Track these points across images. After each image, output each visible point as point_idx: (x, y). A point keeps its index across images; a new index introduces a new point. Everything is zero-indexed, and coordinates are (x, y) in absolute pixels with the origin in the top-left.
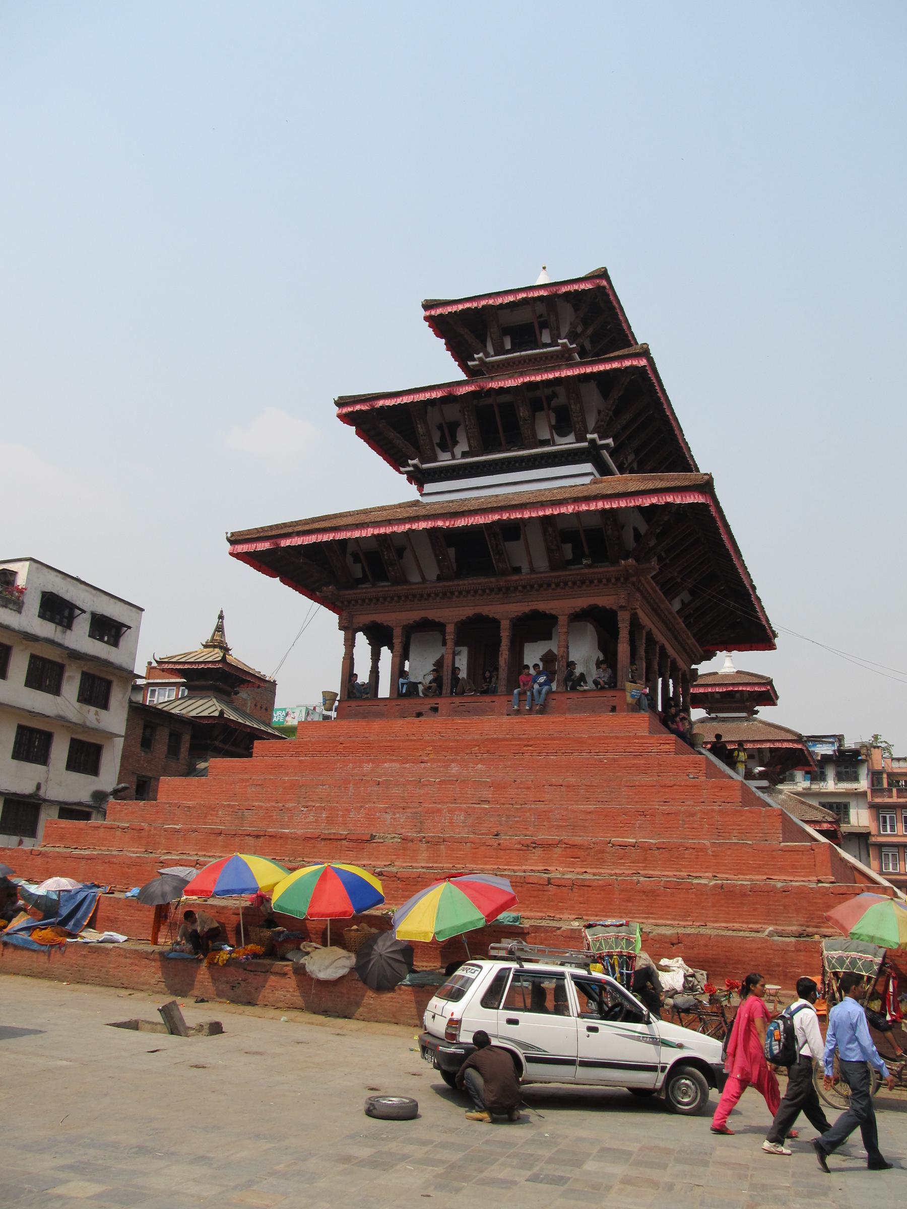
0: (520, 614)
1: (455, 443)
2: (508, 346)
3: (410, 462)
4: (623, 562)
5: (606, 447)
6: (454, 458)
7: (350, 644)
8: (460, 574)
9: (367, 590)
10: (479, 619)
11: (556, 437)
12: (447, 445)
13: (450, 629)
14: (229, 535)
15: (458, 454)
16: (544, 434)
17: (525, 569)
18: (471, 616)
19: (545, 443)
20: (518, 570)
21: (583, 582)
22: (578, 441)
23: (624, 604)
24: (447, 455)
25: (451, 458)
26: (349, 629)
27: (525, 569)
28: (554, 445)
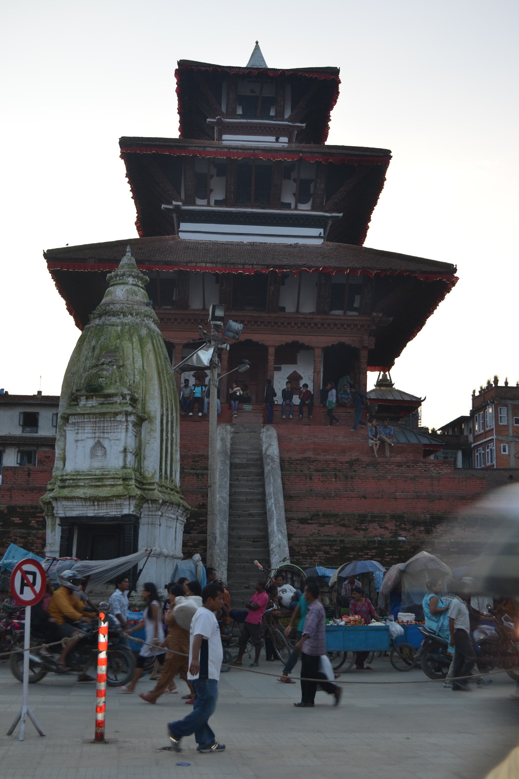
0: (284, 344)
2: (240, 111)
3: (174, 203)
4: (375, 314)
6: (209, 205)
10: (249, 342)
12: (205, 194)
14: (45, 252)
15: (212, 203)
16: (288, 198)
18: (243, 340)
19: (288, 206)
20: (283, 309)
22: (313, 209)
23: (367, 345)
24: (204, 202)
25: (206, 204)
28: (296, 209)
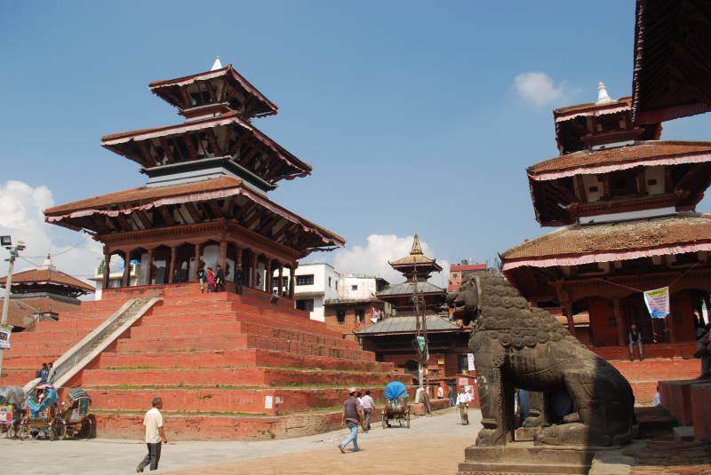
1: (162, 158)
2: (194, 103)
5: (229, 158)
6: (162, 164)
8: (153, 226)
9: (114, 235)
11: (208, 154)
12: (160, 158)
13: (150, 252)
17: (182, 222)
20: (178, 223)
21: (205, 229)
22: (216, 156)
24: (159, 164)
26: (108, 254)
27: (182, 222)
28: (207, 157)
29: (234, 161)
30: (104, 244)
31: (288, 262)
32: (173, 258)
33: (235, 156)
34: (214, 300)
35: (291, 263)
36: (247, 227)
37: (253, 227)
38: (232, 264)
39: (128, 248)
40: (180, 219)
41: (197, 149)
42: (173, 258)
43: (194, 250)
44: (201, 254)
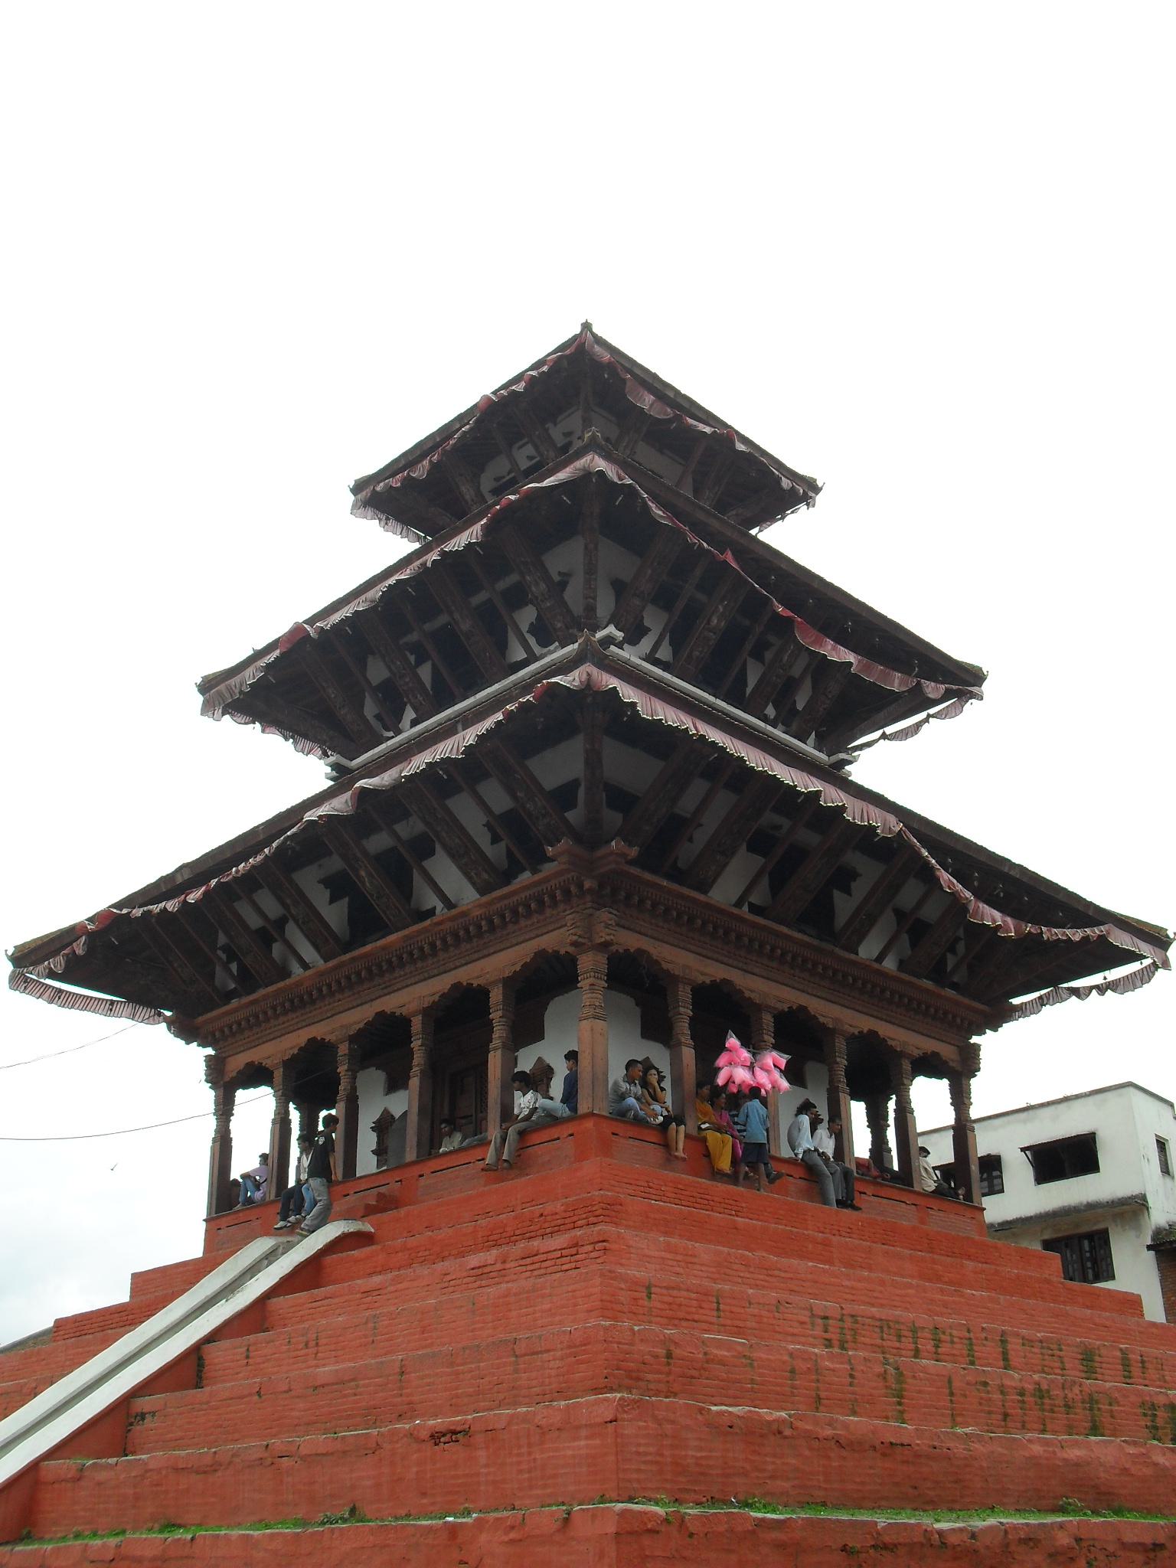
7: (225, 1110)
11: (537, 650)
23: (575, 938)
27: (440, 906)
29: (651, 658)
30: (210, 1051)
31: (929, 1045)
32: (419, 1058)
33: (646, 644)
34: (662, 1239)
35: (947, 1051)
36: (704, 887)
37: (725, 891)
38: (659, 1056)
39: (276, 1050)
40: (432, 901)
41: (503, 647)
42: (419, 1058)
43: (486, 1010)
44: (528, 1031)
